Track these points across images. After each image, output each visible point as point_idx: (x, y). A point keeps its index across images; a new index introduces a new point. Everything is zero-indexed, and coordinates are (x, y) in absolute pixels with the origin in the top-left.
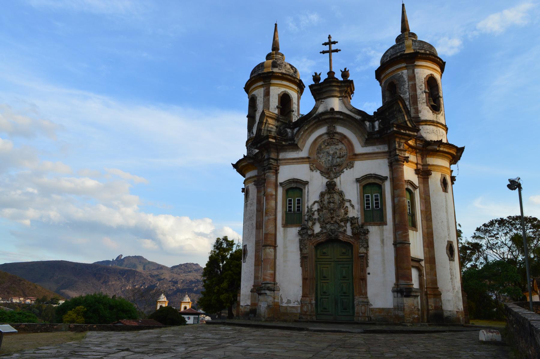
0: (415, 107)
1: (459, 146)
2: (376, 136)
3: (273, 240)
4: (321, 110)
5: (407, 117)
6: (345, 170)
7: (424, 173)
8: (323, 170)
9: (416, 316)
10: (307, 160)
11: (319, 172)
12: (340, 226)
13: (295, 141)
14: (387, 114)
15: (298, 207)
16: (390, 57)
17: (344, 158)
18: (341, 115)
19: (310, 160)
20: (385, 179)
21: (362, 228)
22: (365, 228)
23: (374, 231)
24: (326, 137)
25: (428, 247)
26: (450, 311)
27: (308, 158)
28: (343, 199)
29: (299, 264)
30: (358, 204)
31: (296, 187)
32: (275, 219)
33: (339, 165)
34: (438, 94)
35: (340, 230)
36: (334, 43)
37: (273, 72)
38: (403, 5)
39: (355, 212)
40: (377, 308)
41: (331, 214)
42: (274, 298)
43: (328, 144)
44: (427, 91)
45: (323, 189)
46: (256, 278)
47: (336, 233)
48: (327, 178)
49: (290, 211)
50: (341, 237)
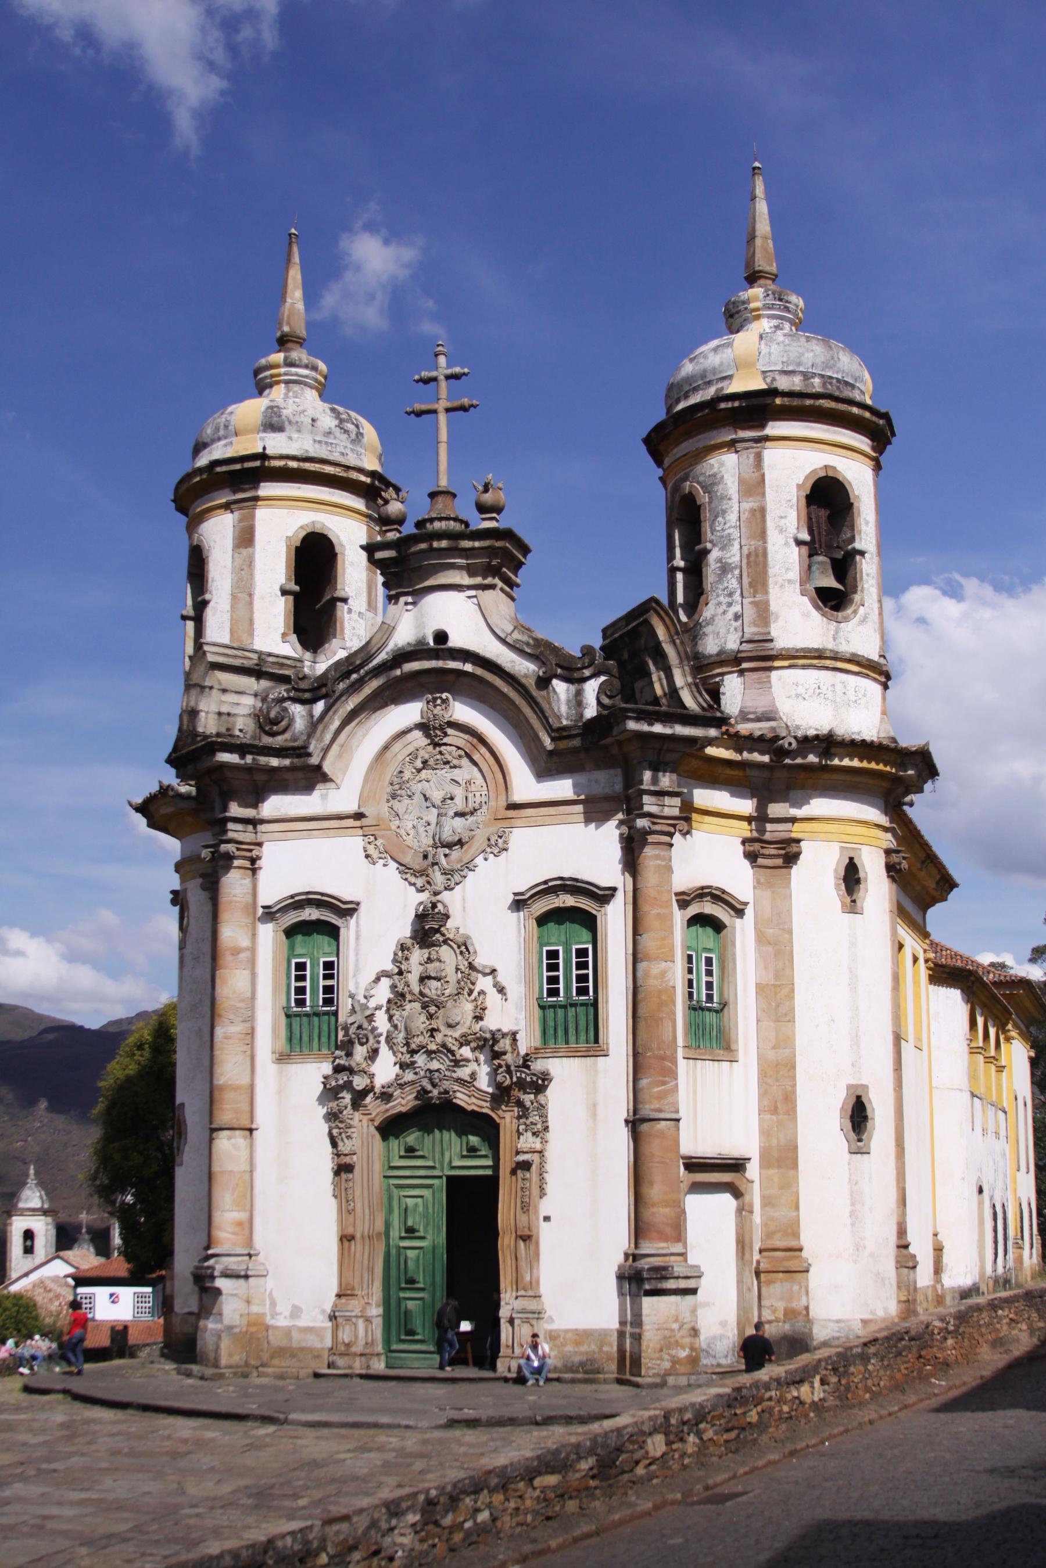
0: (759, 597)
3: (245, 1106)
4: (404, 636)
5: (685, 676)
7: (773, 852)
8: (407, 860)
9: (683, 1354)
10: (358, 823)
11: (393, 865)
12: (457, 1063)
13: (309, 755)
14: (626, 656)
15: (328, 990)
17: (479, 817)
18: (465, 662)
19: (364, 822)
20: (605, 896)
21: (528, 1067)
22: (538, 1066)
24: (418, 738)
25: (774, 1111)
26: (838, 1321)
27: (359, 816)
28: (471, 966)
29: (329, 1188)
30: (520, 982)
31: (316, 921)
32: (251, 1033)
33: (460, 843)
34: (852, 539)
37: (263, 456)
40: (566, 1331)
41: (430, 1017)
42: (248, 1302)
44: (805, 536)
47: (446, 1085)
48: (421, 890)
49: (301, 1003)
50: (462, 1099)
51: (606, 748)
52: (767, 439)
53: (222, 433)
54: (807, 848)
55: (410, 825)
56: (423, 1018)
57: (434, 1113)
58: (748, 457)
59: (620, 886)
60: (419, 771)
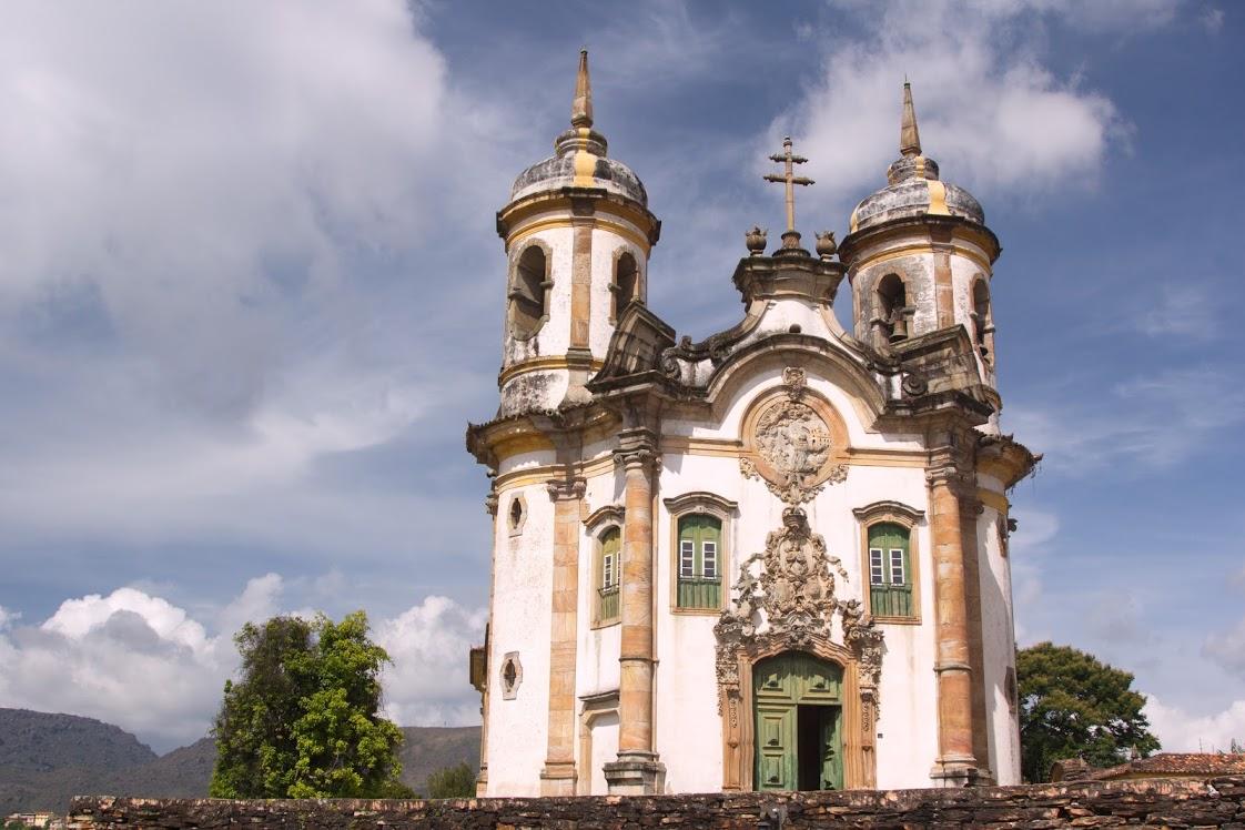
1: (1035, 454)
2: (903, 412)
6: (826, 484)
11: (762, 481)
12: (820, 623)
13: (708, 396)
16: (890, 213)
17: (822, 456)
19: (740, 449)
20: (917, 517)
22: (878, 628)
23: (891, 633)
24: (781, 397)
27: (739, 444)
28: (823, 557)
29: (717, 709)
30: (857, 570)
31: (702, 515)
32: (650, 594)
35: (817, 630)
36: (799, 161)
37: (604, 192)
38: (907, 85)
39: (851, 587)
41: (797, 588)
43: (785, 415)
44: (973, 312)
45: (777, 525)
46: (553, 740)
47: (807, 638)
48: (785, 501)
49: (688, 572)
50: (819, 649)
51: (918, 419)
52: (954, 250)
53: (562, 171)
54: (986, 508)
55: (774, 454)
56: (792, 588)
57: (799, 657)
58: (941, 257)
59: (926, 515)
60: (781, 418)
